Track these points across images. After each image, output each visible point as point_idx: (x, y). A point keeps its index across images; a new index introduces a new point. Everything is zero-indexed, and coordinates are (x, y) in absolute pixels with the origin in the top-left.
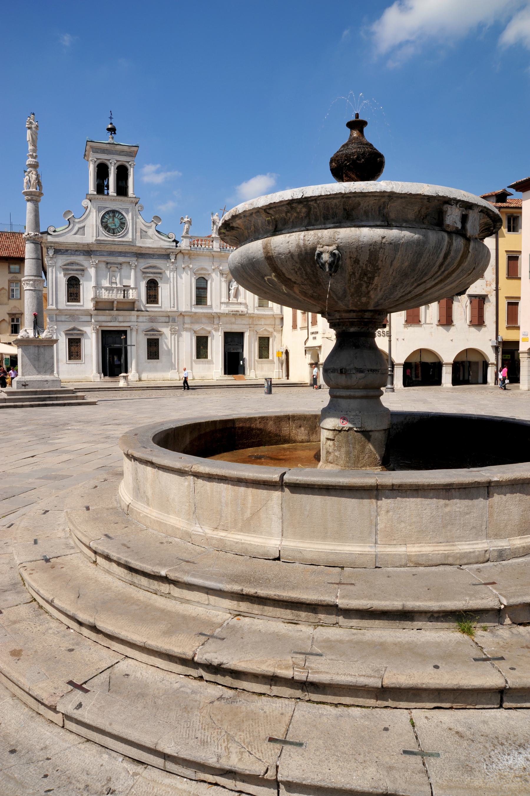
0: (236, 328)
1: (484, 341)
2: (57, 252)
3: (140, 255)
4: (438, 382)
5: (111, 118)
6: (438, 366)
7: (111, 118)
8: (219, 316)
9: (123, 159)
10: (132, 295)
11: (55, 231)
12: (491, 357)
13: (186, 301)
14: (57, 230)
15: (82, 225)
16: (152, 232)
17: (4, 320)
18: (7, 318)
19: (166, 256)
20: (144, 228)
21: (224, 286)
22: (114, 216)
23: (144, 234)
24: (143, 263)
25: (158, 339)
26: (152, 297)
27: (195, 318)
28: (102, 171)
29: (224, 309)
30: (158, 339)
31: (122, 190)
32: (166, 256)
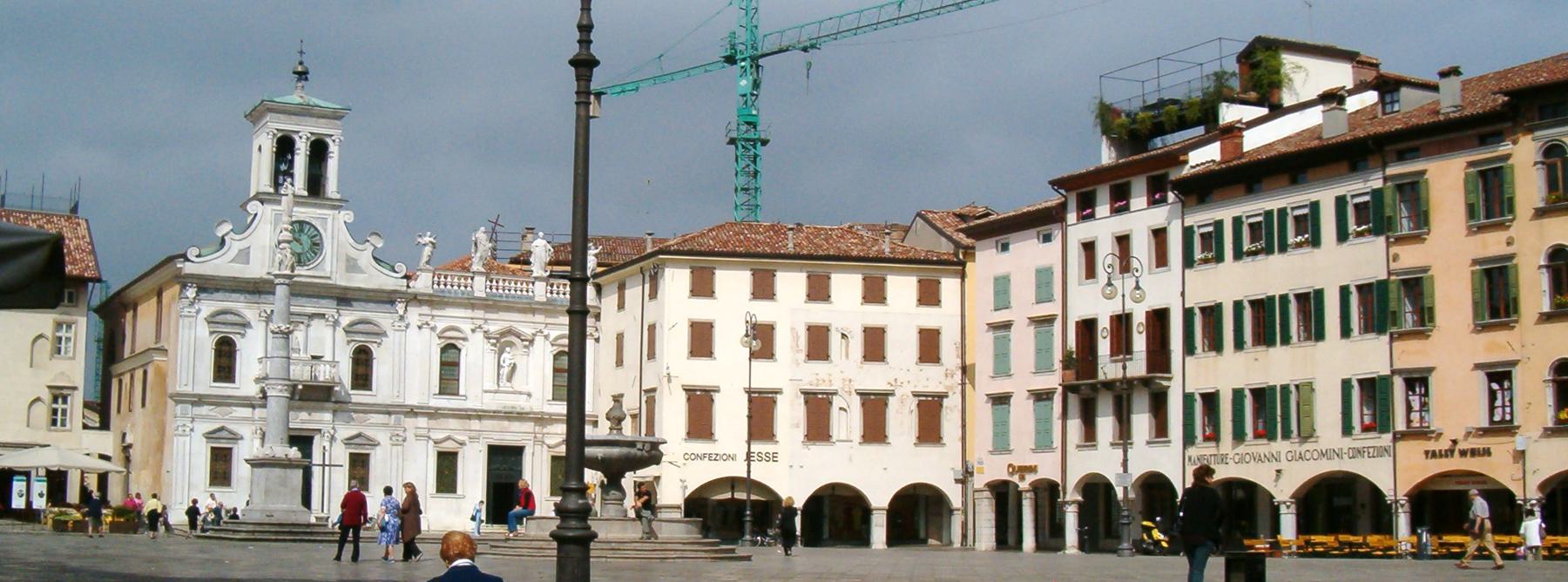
0: (509, 439)
1: (935, 468)
2: (201, 289)
3: (345, 298)
4: (861, 537)
5: (301, 52)
6: (866, 511)
7: (301, 52)
8: (480, 415)
9: (321, 128)
10: (324, 374)
11: (199, 256)
12: (955, 499)
13: (421, 386)
14: (204, 252)
15: (244, 244)
16: (365, 258)
17: (38, 399)
18: (46, 395)
19: (387, 299)
20: (353, 253)
21: (491, 358)
22: (301, 230)
23: (352, 266)
24: (347, 317)
25: (368, 455)
26: (362, 378)
27: (434, 414)
28: (285, 146)
29: (491, 403)
30: (368, 455)
31: (315, 185)
32: (387, 299)
